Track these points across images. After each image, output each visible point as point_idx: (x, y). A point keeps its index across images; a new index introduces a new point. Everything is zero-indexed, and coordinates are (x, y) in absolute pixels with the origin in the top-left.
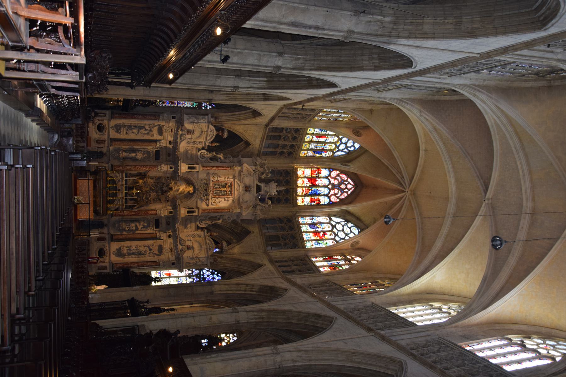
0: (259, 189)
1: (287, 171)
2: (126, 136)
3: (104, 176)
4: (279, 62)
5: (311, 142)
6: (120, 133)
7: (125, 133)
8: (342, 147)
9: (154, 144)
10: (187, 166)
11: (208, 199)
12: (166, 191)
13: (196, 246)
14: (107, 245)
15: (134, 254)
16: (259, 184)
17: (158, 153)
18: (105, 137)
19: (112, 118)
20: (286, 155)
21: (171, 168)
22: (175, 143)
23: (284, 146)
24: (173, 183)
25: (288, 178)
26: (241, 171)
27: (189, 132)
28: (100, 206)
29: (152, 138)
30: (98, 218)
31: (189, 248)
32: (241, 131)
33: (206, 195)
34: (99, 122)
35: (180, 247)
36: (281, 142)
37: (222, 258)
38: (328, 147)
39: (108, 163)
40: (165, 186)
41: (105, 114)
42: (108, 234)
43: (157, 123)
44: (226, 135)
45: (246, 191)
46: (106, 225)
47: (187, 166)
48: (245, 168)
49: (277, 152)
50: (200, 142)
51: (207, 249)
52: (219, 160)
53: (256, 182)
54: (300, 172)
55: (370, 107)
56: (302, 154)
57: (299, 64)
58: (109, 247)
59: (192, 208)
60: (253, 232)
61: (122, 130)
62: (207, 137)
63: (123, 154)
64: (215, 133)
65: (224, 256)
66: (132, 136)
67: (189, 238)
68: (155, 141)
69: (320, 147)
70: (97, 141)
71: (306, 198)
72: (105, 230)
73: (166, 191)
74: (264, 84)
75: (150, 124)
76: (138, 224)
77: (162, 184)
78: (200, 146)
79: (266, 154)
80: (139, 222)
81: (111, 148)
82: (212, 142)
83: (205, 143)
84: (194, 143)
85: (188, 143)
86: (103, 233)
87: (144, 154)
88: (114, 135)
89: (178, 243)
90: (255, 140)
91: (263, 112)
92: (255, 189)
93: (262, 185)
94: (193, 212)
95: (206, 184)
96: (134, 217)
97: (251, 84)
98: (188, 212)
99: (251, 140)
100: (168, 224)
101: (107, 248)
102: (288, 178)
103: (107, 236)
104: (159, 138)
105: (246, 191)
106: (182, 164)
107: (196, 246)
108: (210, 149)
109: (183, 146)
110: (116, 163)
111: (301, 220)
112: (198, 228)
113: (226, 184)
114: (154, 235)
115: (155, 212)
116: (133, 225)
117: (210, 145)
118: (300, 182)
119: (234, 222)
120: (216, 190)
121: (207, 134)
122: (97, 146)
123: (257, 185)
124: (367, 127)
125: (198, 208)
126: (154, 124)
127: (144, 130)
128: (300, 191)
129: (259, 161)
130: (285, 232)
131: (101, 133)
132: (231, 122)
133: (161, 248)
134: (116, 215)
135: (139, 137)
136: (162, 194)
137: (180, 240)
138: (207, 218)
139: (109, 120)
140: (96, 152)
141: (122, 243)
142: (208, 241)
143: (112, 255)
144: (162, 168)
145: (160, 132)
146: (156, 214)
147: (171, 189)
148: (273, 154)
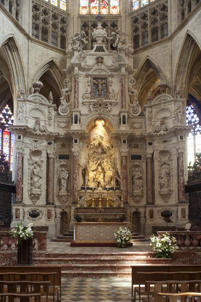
0: (100, 49)
1: (83, 26)
2: (42, 188)
3: (82, 210)
6: (40, 195)
7: (39, 190)
9: (51, 161)
10: (74, 124)
11: (111, 103)
12: (103, 149)
13: (161, 116)
14: (158, 209)
15: (168, 180)
16: (95, 49)
17: (61, 157)
18: (44, 210)
19: (21, 202)
20: (65, 25)
21: (76, 141)
22: (53, 139)
23: (54, 26)
24: (94, 142)
25: (90, 24)
26: (80, 68)
27: (37, 122)
28: (115, 215)
29: (45, 163)
30: (128, 218)
31: (163, 123)
32: (36, 68)
33: (106, 105)
34: (27, 216)
35: (162, 132)
36: (50, 29)
37: (175, 87)
39: (70, 207)
40: (96, 150)
41: (16, 209)
42: (145, 207)
43: (26, 157)
44: (41, 83)
45: (102, 62)
46: (137, 210)
47: (74, 124)
48: (77, 62)
49: (61, 36)
50: (49, 113)
51: (165, 103)
52: (69, 93)
53: (93, 52)
54: (84, 12)
58: (159, 206)
59: (120, 119)
60: (148, 56)
61: (34, 192)
62: (43, 104)
63: (63, 192)
64: (37, 94)
65: (174, 84)
66: (43, 182)
67: (153, 123)
68: (48, 158)
70: (49, 218)
71: (111, 5)
72: (141, 210)
73: (103, 149)
75: (29, 163)
76: (136, 177)
77: (95, 154)
78: (53, 113)
79: (63, 45)
80: (134, 176)
81: (57, 203)
83: (49, 107)
84: (50, 119)
85: (50, 125)
86: (145, 212)
87: (62, 170)
88: (42, 201)
89: (158, 134)
90: (47, 55)
92: (100, 54)
93: (95, 46)
94: (124, 117)
95: (94, 105)
96: (129, 181)
98: (124, 123)
99: (47, 59)
100: (136, 147)
101: (161, 208)
102: (90, 24)
103: (148, 209)
104: (44, 154)
105: (102, 62)
106: (72, 129)
107: (161, 116)
108: (57, 102)
109: (52, 129)
110: (71, 200)
111: (136, 7)
112: (142, 115)
113: (94, 84)
114: (149, 161)
115: (124, 158)
116: (137, 182)
117: (52, 102)
118: (94, 12)
119: (137, 78)
120: (101, 95)
121: (38, 103)
122: (53, 218)
123: (95, 51)
125: (120, 112)
126: (29, 160)
127: (34, 170)
128: (104, 12)
129: (69, 48)
130: (148, 22)
131: (40, 214)
132: (26, 78)
133: (164, 152)
134: (127, 199)
135: (44, 174)
136: (105, 153)
137: (155, 132)
138: (131, 105)
139: (24, 206)
140: (62, 219)
141: (156, 193)
142: (157, 103)
143: (167, 204)
144: (76, 150)
145: (36, 153)
146: (126, 157)
147: (100, 144)
148: (63, 40)
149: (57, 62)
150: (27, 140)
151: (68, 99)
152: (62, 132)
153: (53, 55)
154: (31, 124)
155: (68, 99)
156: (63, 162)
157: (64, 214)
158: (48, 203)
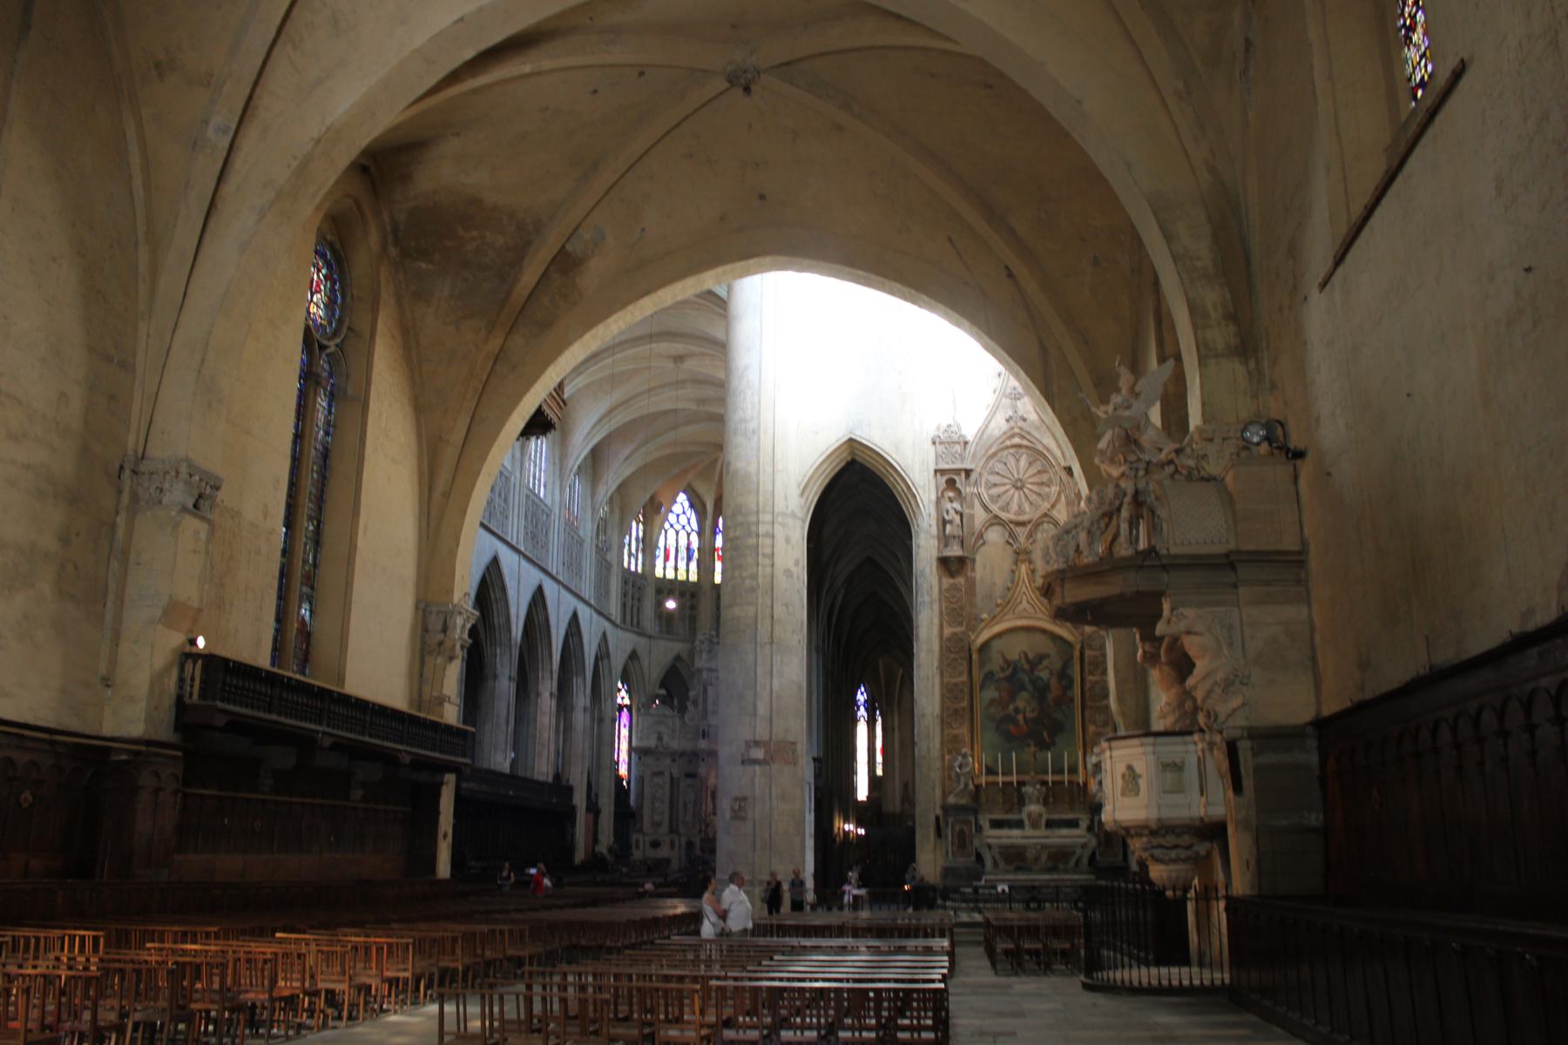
4: (546, 695)
5: (676, 569)
8: (683, 520)
17: (688, 775)
22: (675, 756)
27: (660, 739)
38: (683, 542)
44: (663, 692)
55: (617, 511)
56: (693, 577)
57: (547, 675)
68: (672, 778)
69: (683, 554)
74: (580, 680)
78: (678, 722)
79: (693, 631)
81: (682, 830)
82: (672, 708)
88: (665, 828)
91: (629, 650)
97: (581, 696)
104: (667, 774)
109: (675, 745)
124: (652, 498)
135: (667, 800)
145: (659, 774)
149: (685, 656)
150: (649, 760)
151: (695, 703)
152: (687, 746)
153: (677, 647)
154: (652, 743)
155: (695, 703)
156: (690, 781)
157: (690, 844)
158: (671, 831)
